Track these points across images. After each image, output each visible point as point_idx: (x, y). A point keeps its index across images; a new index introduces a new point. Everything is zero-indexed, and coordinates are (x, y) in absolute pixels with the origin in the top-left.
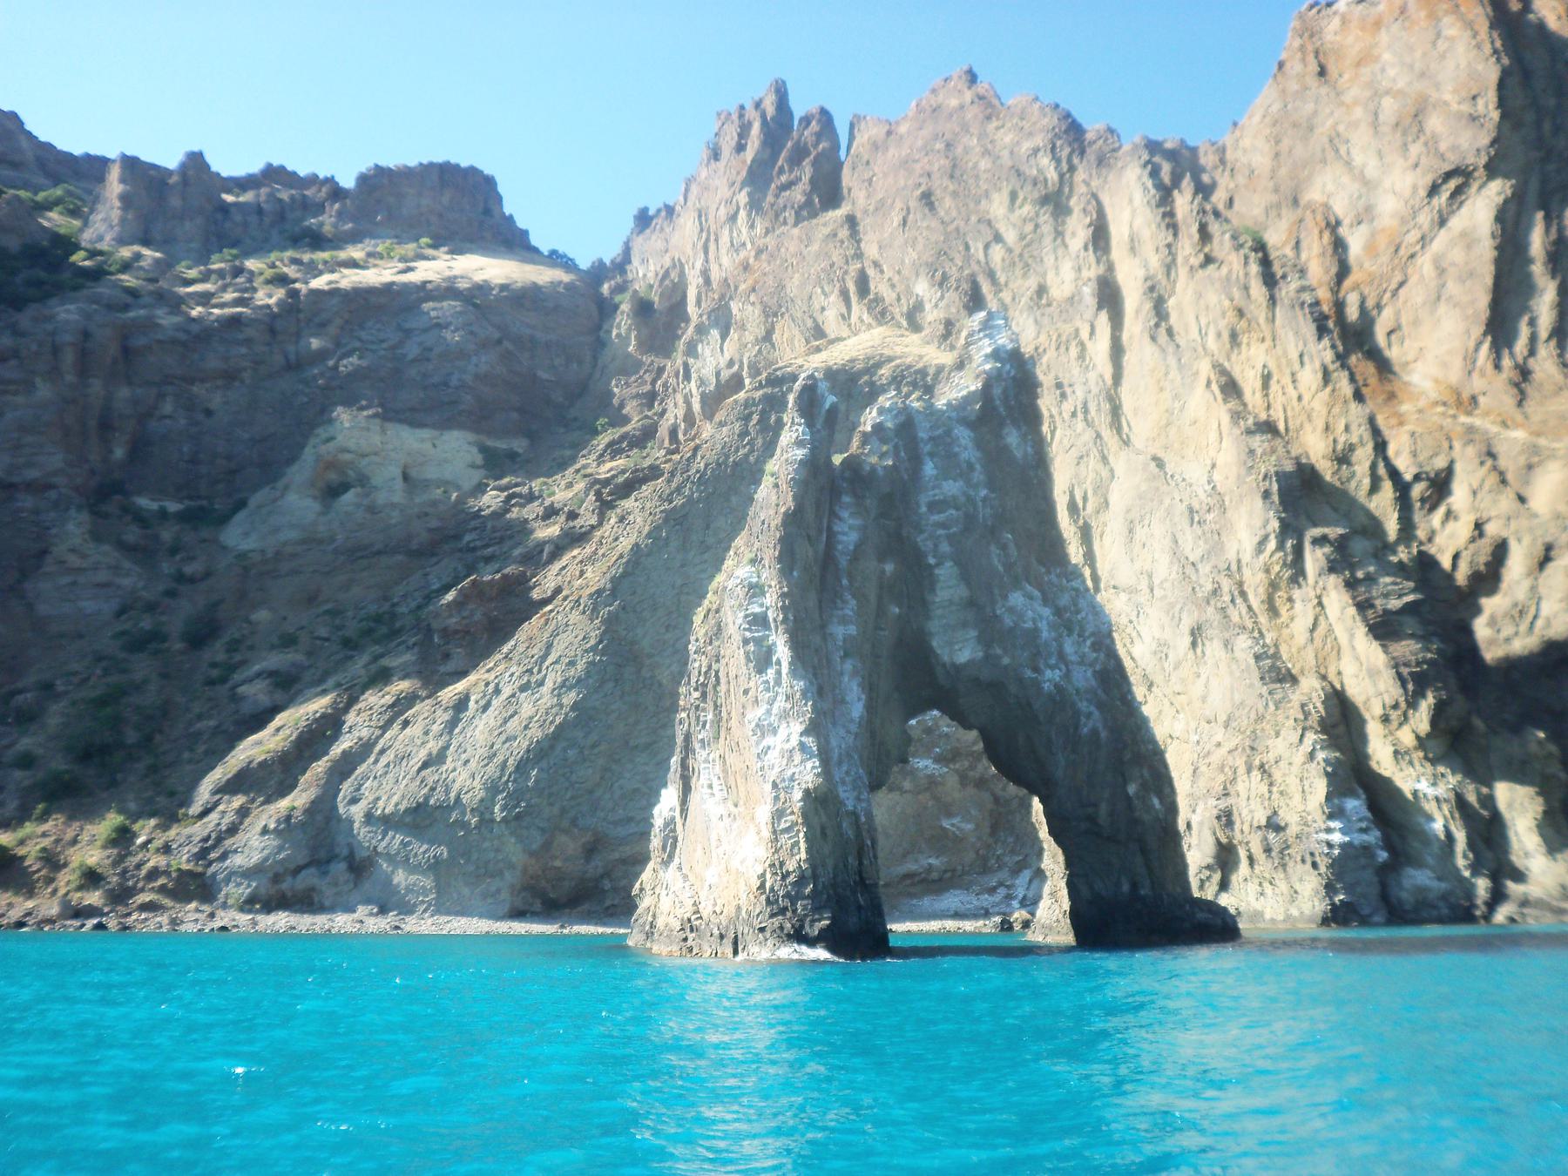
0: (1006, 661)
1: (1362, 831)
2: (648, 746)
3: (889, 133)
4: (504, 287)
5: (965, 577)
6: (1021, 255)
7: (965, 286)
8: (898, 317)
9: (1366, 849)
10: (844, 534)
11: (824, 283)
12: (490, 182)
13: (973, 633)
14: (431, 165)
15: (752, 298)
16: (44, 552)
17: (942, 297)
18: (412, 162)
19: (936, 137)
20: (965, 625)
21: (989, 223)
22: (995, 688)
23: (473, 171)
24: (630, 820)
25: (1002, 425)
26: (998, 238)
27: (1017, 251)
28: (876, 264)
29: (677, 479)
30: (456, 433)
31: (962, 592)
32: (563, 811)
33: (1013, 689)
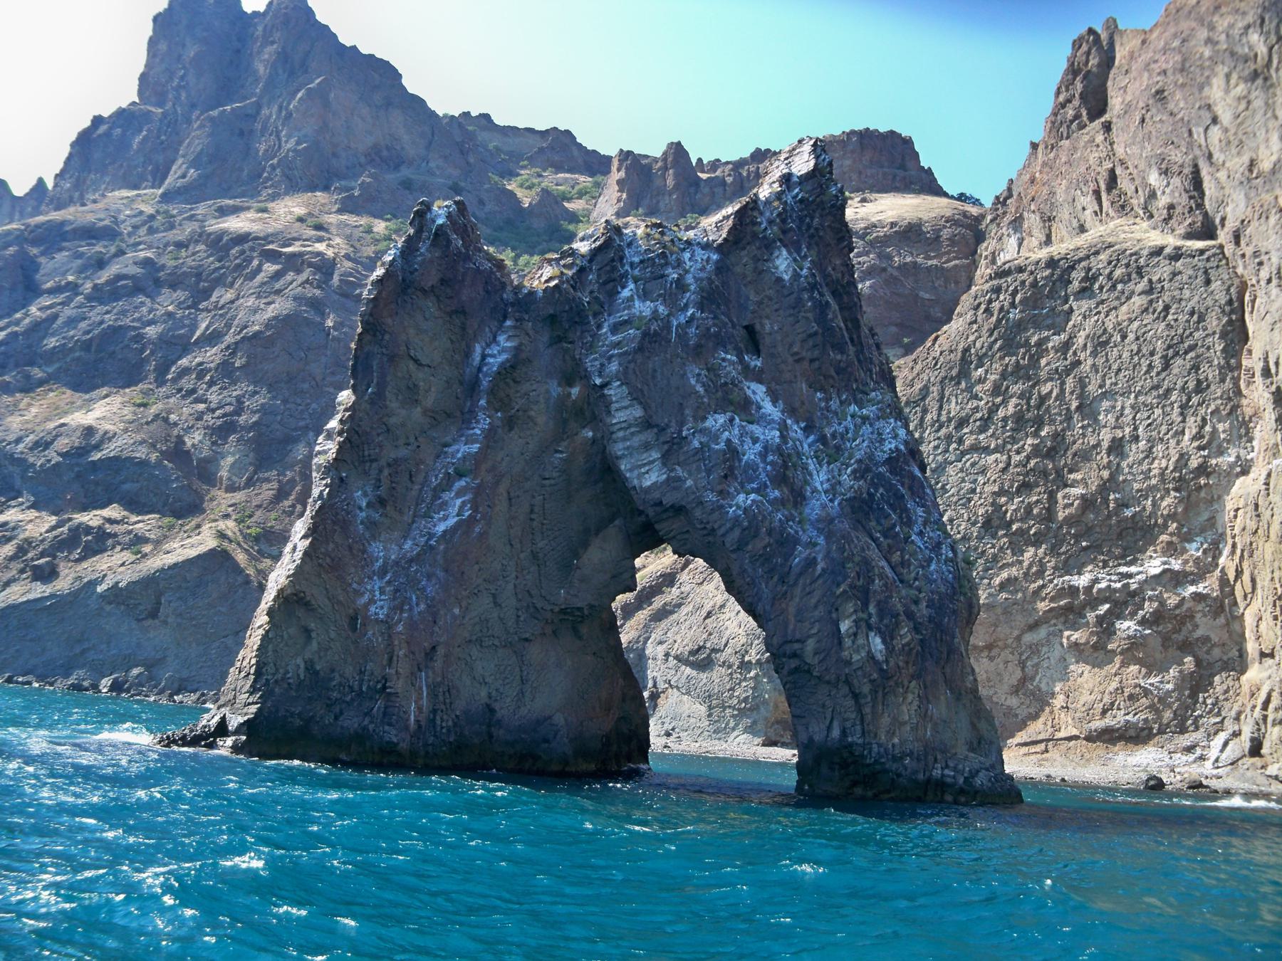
0: (689, 483)
3: (1144, 42)
4: (893, 224)
5: (637, 396)
6: (1235, 134)
7: (1187, 170)
8: (1136, 208)
10: (493, 356)
11: (1082, 185)
12: (908, 142)
13: (655, 455)
14: (853, 132)
15: (1033, 207)
17: (1168, 184)
18: (837, 132)
19: (1175, 36)
20: (647, 447)
21: (1209, 107)
22: (678, 510)
26: (1215, 120)
27: (1233, 131)
28: (1122, 162)
29: (919, 367)
31: (638, 412)
33: (698, 513)
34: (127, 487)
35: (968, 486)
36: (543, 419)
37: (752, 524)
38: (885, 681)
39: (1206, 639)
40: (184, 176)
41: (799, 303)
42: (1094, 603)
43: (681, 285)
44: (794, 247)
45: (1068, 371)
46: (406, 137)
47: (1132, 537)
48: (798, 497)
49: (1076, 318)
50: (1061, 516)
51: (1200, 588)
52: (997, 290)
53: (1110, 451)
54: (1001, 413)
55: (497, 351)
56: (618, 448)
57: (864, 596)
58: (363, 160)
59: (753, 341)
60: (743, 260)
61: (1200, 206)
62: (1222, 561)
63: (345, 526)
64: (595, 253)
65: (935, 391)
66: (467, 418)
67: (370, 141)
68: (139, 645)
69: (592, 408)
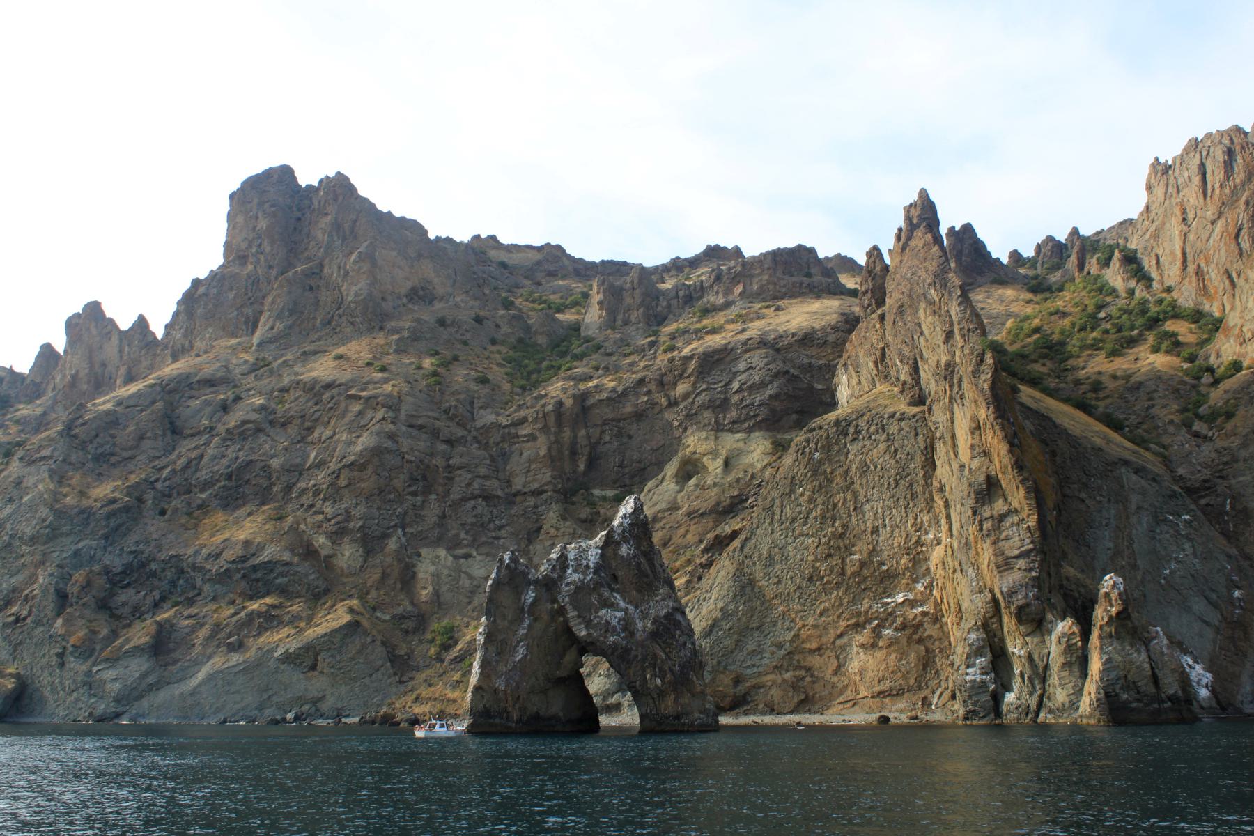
1: (986, 674)
2: (758, 628)
4: (794, 335)
5: (575, 608)
9: (983, 682)
14: (768, 253)
16: (540, 528)
18: (757, 254)
22: (592, 643)
23: (800, 248)
24: (753, 666)
25: (618, 544)
30: (757, 434)
31: (576, 613)
32: (719, 663)
34: (279, 581)
35: (799, 557)
36: (545, 617)
37: (615, 646)
38: (662, 693)
39: (930, 637)
40: (272, 328)
41: (630, 564)
42: (869, 621)
43: (588, 566)
44: (627, 542)
45: (848, 488)
46: (436, 280)
47: (887, 581)
48: (632, 634)
49: (851, 456)
50: (849, 572)
51: (925, 609)
52: (808, 441)
53: (872, 533)
54: (814, 514)
55: (530, 596)
56: (571, 624)
57: (654, 666)
58: (405, 300)
59: (615, 578)
60: (610, 550)
61: (918, 383)
62: (934, 592)
63: (489, 663)
64: (558, 558)
65: (778, 502)
66: (522, 621)
67: (409, 285)
68: (306, 690)
69: (562, 611)
